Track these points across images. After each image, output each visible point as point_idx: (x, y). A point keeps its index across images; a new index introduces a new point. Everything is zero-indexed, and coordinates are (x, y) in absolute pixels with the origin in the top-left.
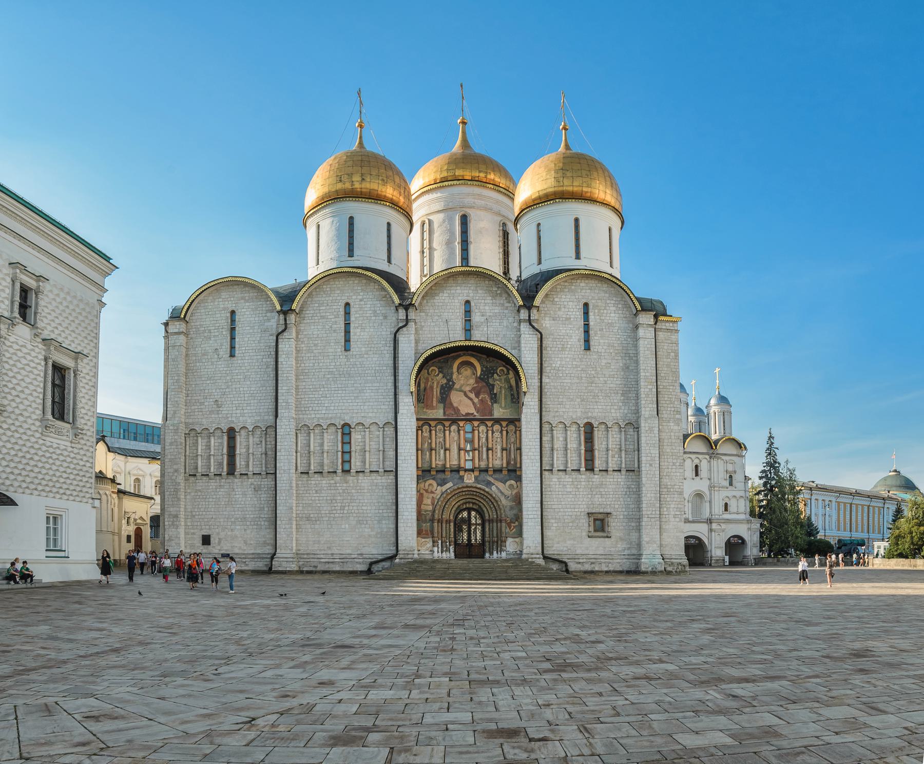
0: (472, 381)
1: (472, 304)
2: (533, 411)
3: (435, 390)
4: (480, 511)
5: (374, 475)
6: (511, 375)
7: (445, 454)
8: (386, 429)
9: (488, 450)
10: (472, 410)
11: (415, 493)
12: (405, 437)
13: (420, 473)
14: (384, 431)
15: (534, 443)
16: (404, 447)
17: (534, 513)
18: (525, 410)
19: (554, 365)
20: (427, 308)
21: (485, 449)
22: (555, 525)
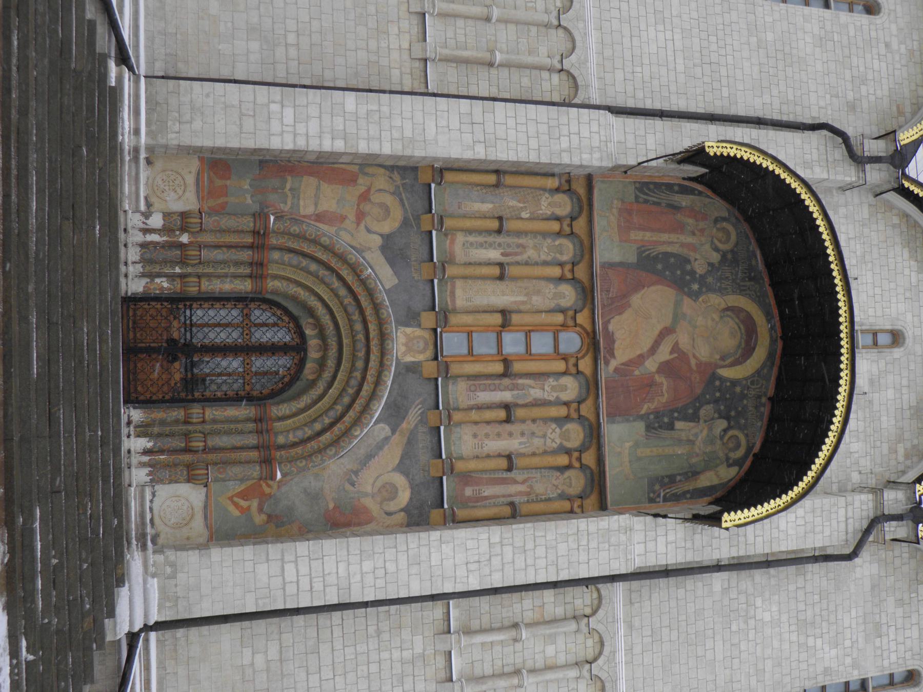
0: (704, 352)
1: (897, 352)
2: (639, 549)
3: (673, 237)
4: (299, 385)
5: (410, 25)
6: (727, 474)
7: (489, 264)
8: (555, 78)
9: (507, 407)
10: (622, 355)
11: (363, 147)
12: (543, 128)
13: (425, 177)
14: (550, 70)
15: (542, 563)
16: (511, 122)
17: (305, 583)
18: (640, 523)
19: (759, 602)
20: (881, 227)
21: (506, 396)
22: (259, 660)
